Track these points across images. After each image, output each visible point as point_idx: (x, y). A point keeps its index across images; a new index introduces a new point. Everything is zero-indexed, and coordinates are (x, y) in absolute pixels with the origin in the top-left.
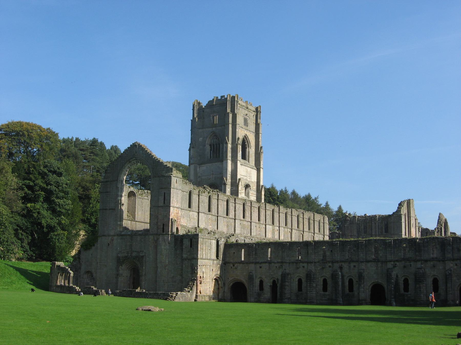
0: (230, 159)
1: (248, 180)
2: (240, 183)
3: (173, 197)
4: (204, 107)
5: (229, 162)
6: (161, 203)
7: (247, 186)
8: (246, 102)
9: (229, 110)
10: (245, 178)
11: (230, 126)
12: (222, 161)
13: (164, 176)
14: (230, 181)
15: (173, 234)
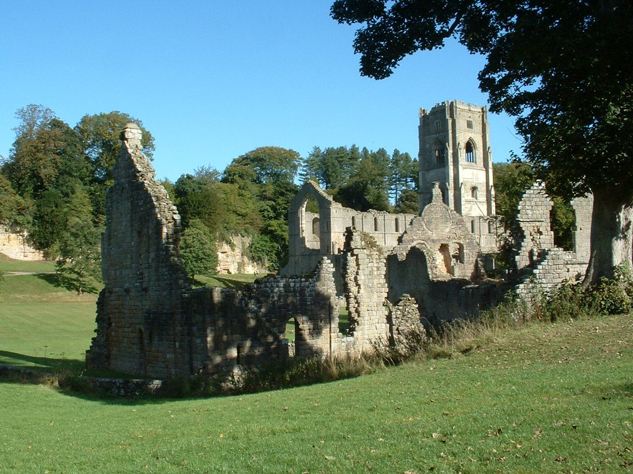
0: (452, 164)
1: (475, 182)
2: (463, 186)
3: (334, 224)
4: (428, 114)
5: (451, 168)
6: (325, 230)
7: (474, 189)
8: (469, 105)
9: (448, 117)
10: (470, 180)
11: (450, 132)
12: (444, 167)
13: (326, 208)
14: (453, 185)
15: (333, 254)
